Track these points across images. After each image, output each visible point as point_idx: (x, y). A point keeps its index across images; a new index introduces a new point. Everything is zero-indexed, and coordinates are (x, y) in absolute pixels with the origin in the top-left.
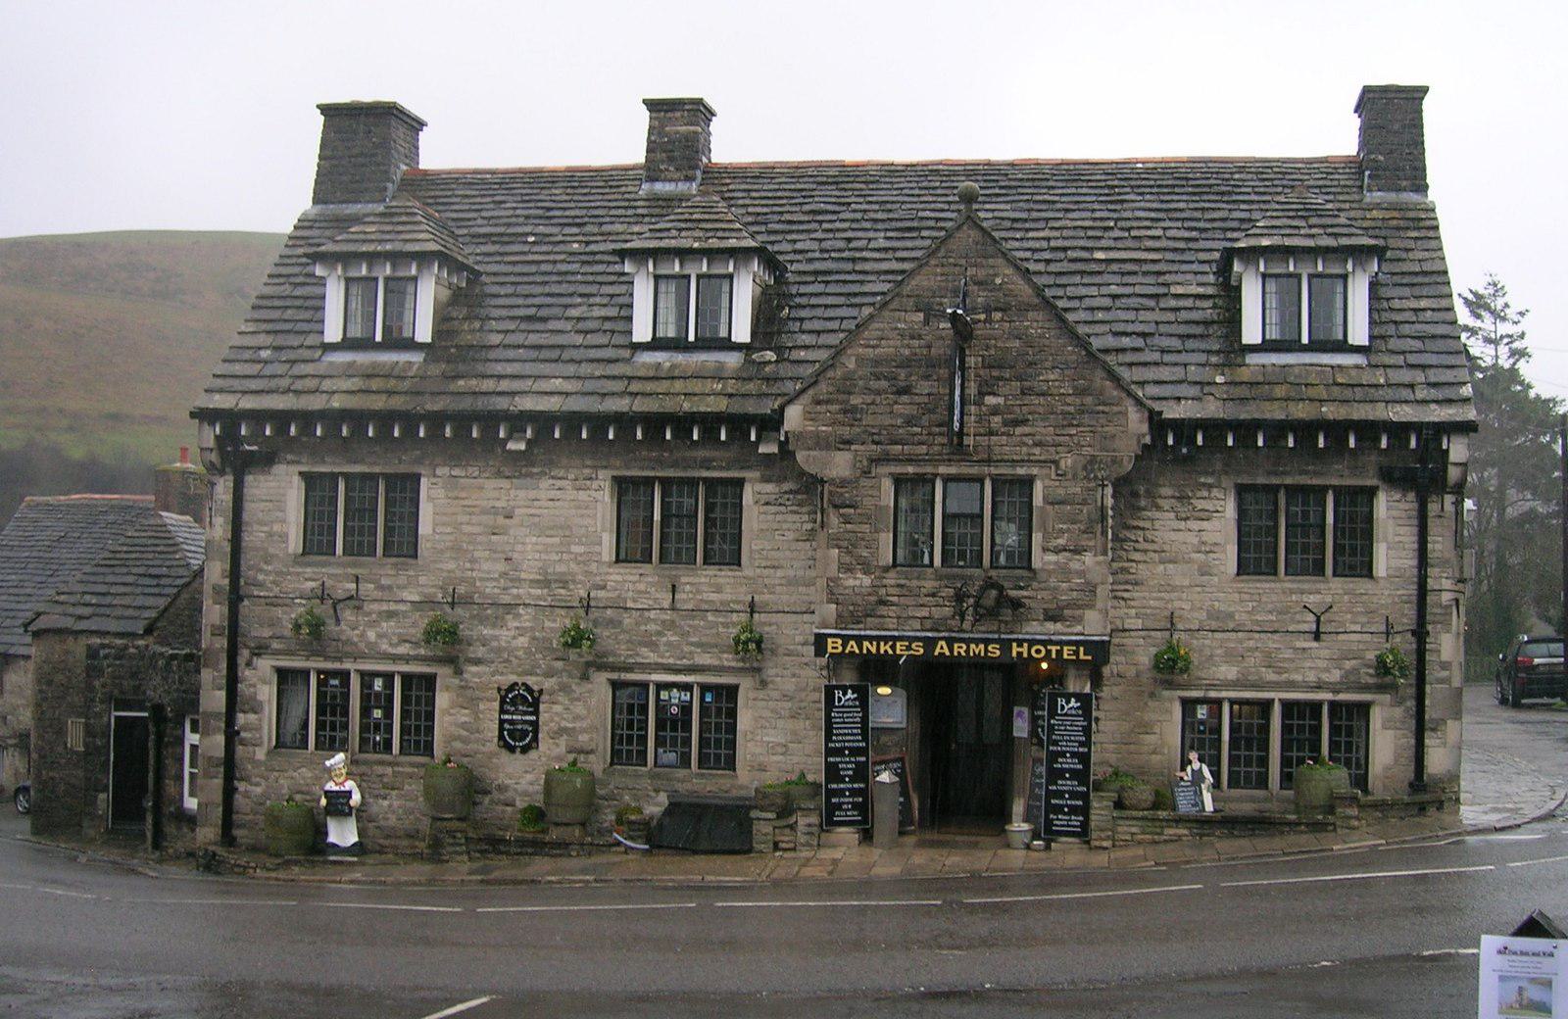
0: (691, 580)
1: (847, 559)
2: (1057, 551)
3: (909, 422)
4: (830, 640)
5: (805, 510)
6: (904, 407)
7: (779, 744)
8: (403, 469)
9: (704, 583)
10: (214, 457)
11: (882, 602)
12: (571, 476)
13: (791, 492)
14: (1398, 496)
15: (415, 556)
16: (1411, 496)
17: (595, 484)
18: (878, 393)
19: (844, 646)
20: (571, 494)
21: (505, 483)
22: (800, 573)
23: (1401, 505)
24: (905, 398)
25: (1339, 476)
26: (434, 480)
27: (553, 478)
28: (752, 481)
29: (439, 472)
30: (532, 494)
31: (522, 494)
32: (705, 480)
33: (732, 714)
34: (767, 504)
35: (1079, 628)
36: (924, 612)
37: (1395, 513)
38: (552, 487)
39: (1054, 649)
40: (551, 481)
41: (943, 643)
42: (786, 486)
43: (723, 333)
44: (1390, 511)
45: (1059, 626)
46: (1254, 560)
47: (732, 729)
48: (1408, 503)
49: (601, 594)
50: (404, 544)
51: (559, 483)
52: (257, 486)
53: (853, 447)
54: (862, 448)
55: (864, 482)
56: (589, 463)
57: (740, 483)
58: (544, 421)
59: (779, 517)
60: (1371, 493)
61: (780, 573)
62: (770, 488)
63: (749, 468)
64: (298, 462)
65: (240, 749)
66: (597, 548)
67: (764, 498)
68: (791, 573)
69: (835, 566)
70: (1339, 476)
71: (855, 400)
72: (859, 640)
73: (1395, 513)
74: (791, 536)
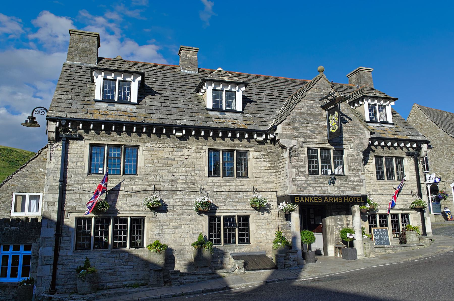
0: (235, 182)
1: (297, 172)
2: (352, 170)
3: (312, 131)
4: (295, 197)
5: (267, 160)
6: (310, 127)
7: (265, 234)
8: (132, 143)
9: (237, 183)
10: (53, 135)
11: (309, 185)
12: (194, 148)
13: (263, 155)
14: (410, 160)
15: (136, 174)
16: (412, 159)
17: (202, 151)
18: (303, 123)
19: (300, 199)
20: (194, 154)
21: (171, 150)
22: (267, 180)
23: (410, 162)
24: (310, 125)
25: (397, 153)
26: (145, 148)
27: (188, 148)
28: (251, 151)
29: (147, 145)
30: (181, 154)
31: (177, 153)
32: (237, 150)
33: (248, 225)
34: (256, 158)
35: (359, 192)
36: (320, 189)
37: (409, 164)
38: (188, 151)
39: (355, 198)
40: (187, 150)
41: (326, 198)
42: (262, 153)
43: (233, 108)
44: (408, 163)
45: (355, 192)
46: (380, 177)
47: (248, 230)
48: (412, 161)
49: (205, 187)
50: (131, 170)
51: (190, 150)
52: (74, 146)
53: (297, 139)
54: (299, 139)
55: (301, 149)
56: (200, 144)
57: (247, 152)
58: (188, 129)
59: (260, 163)
60: (402, 158)
61: (261, 179)
62: (257, 153)
63: (251, 147)
64: (90, 140)
65: (61, 253)
66: (203, 172)
67: (255, 157)
68: (265, 179)
69: (294, 174)
70: (397, 153)
71: (296, 125)
72: (304, 197)
73: (409, 164)
74: (264, 168)
